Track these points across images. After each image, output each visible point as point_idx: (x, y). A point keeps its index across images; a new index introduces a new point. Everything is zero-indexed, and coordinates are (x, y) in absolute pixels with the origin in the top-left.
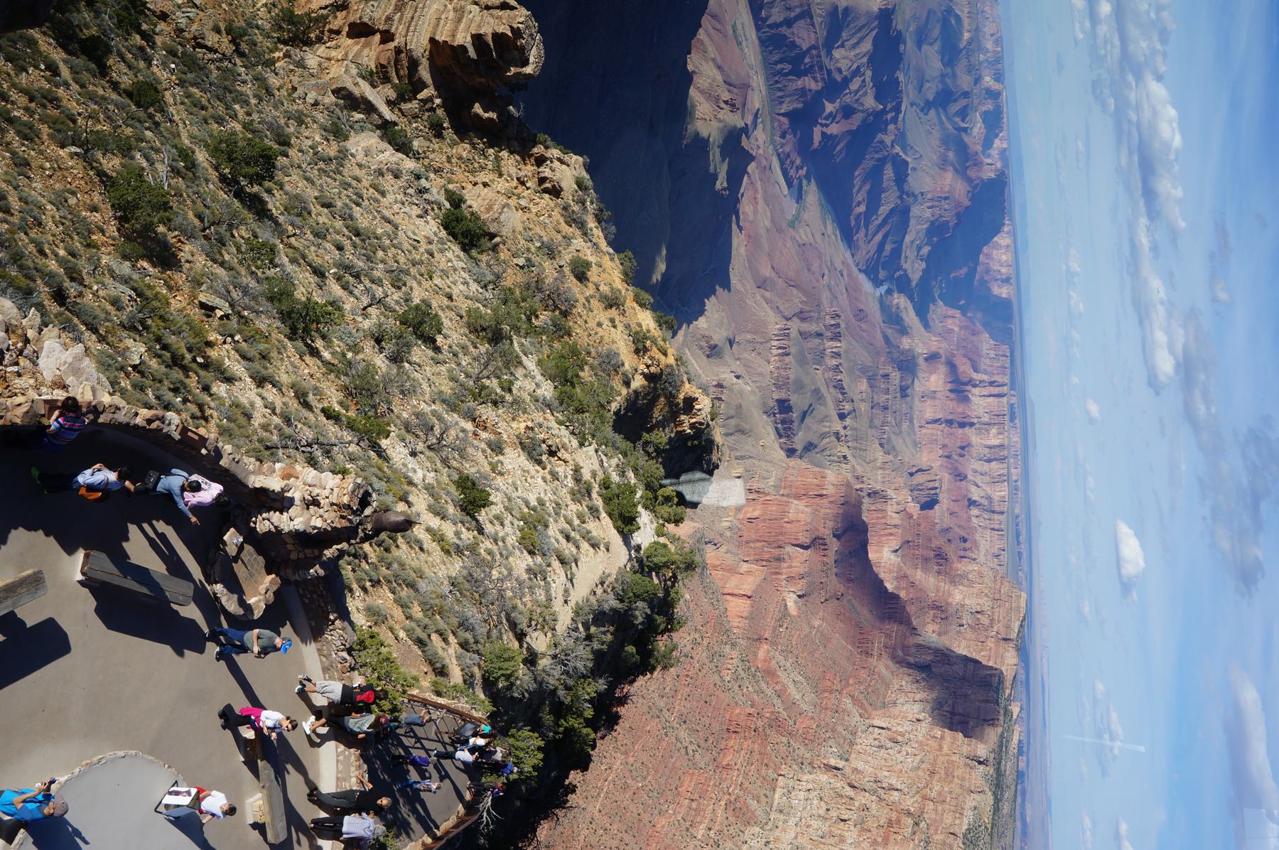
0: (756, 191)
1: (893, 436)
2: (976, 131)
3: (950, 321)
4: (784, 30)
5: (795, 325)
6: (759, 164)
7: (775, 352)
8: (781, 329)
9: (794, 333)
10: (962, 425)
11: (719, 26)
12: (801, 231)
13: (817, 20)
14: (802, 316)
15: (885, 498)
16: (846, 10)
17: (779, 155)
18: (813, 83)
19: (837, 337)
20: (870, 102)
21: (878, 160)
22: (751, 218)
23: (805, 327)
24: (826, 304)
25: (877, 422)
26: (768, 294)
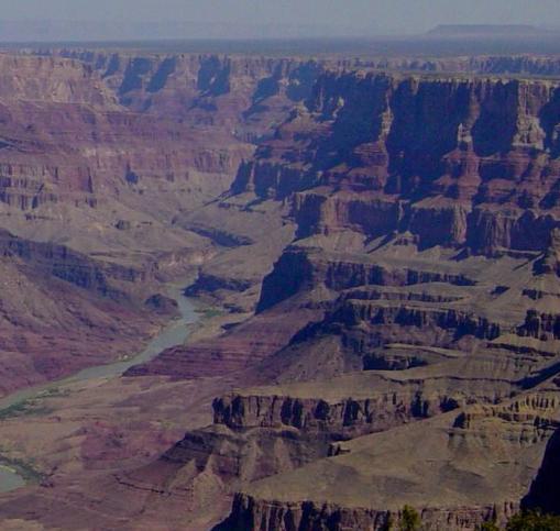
23: (248, 469)
24: (205, 421)
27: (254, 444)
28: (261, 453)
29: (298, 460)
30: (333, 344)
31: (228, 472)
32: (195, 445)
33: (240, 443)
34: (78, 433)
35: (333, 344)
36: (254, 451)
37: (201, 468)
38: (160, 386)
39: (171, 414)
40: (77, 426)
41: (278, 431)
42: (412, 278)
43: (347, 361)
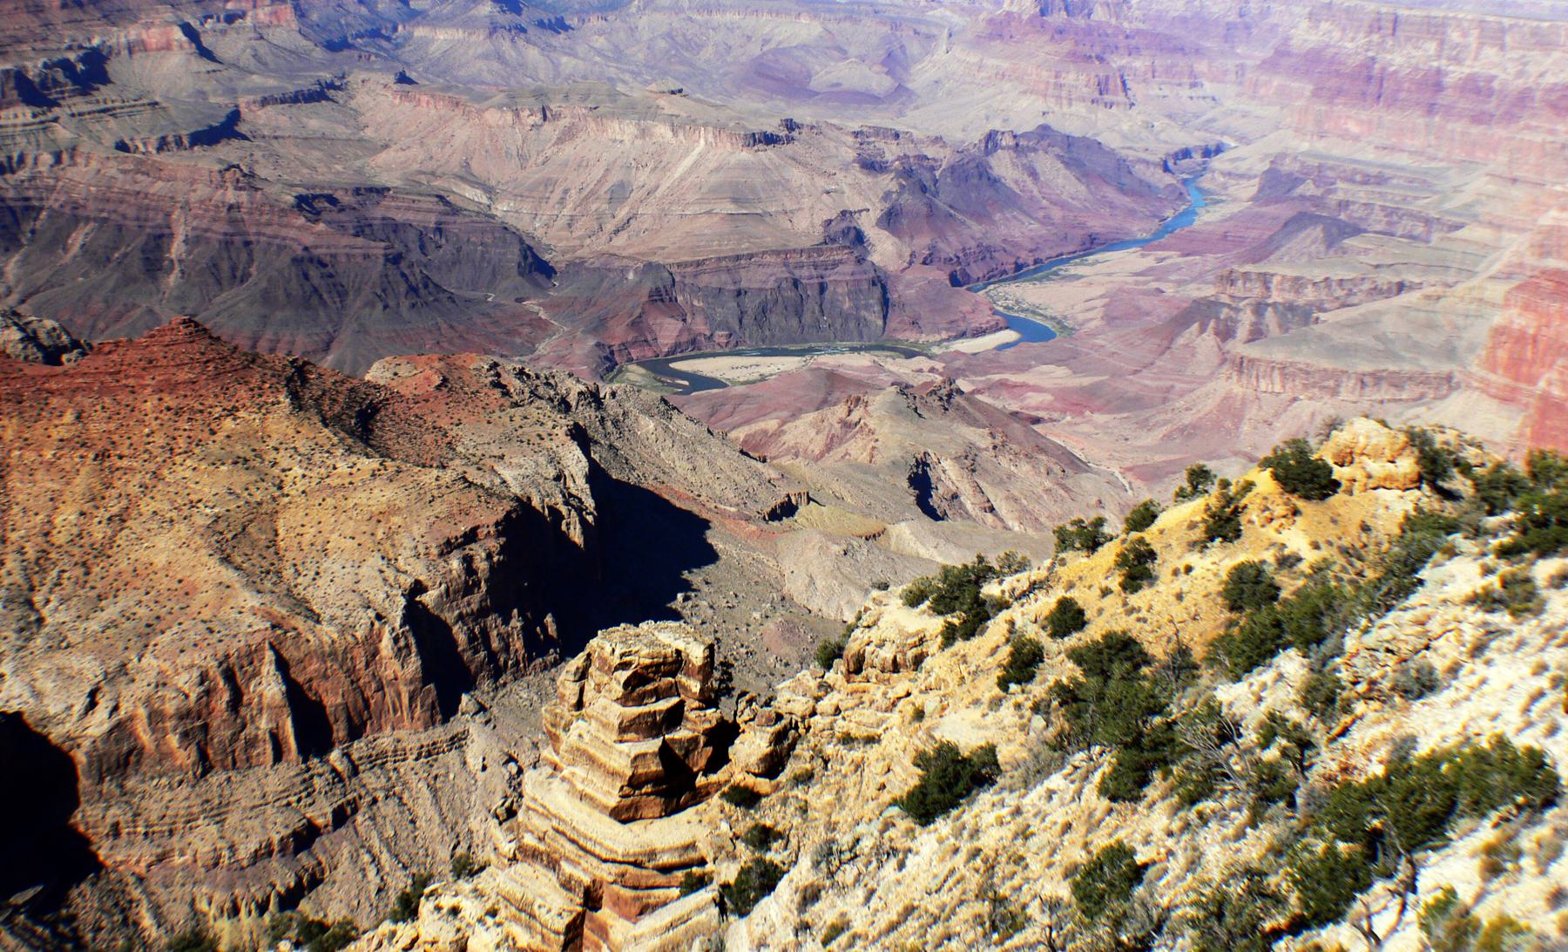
0: (1003, 384)
1: (1447, 206)
2: (957, 20)
3: (1262, 91)
4: (751, 304)
5: (1237, 347)
6: (961, 372)
7: (1278, 388)
8: (1240, 372)
9: (1252, 351)
10: (1438, 87)
11: (728, 408)
12: (1081, 317)
13: (745, 248)
14: (1226, 333)
15: (1551, 231)
16: (735, 201)
17: (948, 340)
18: (840, 268)
19: (1265, 280)
20: (888, 182)
21: (981, 176)
22: (1049, 397)
23: (1242, 332)
24: (1208, 291)
25: (1420, 229)
26: (1178, 386)
27: (1248, 311)
28: (1253, 319)
29: (1284, 327)
30: (1317, 232)
31: (1226, 333)
32: (1199, 312)
33: (1237, 310)
34: (1102, 296)
35: (1317, 232)
36: (1247, 318)
37: (1203, 330)
38: (1169, 261)
39: (1180, 283)
40: (1101, 291)
41: (1270, 301)
42: (1381, 180)
43: (1329, 246)
